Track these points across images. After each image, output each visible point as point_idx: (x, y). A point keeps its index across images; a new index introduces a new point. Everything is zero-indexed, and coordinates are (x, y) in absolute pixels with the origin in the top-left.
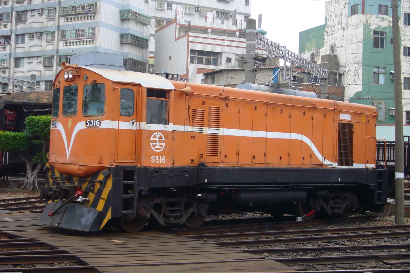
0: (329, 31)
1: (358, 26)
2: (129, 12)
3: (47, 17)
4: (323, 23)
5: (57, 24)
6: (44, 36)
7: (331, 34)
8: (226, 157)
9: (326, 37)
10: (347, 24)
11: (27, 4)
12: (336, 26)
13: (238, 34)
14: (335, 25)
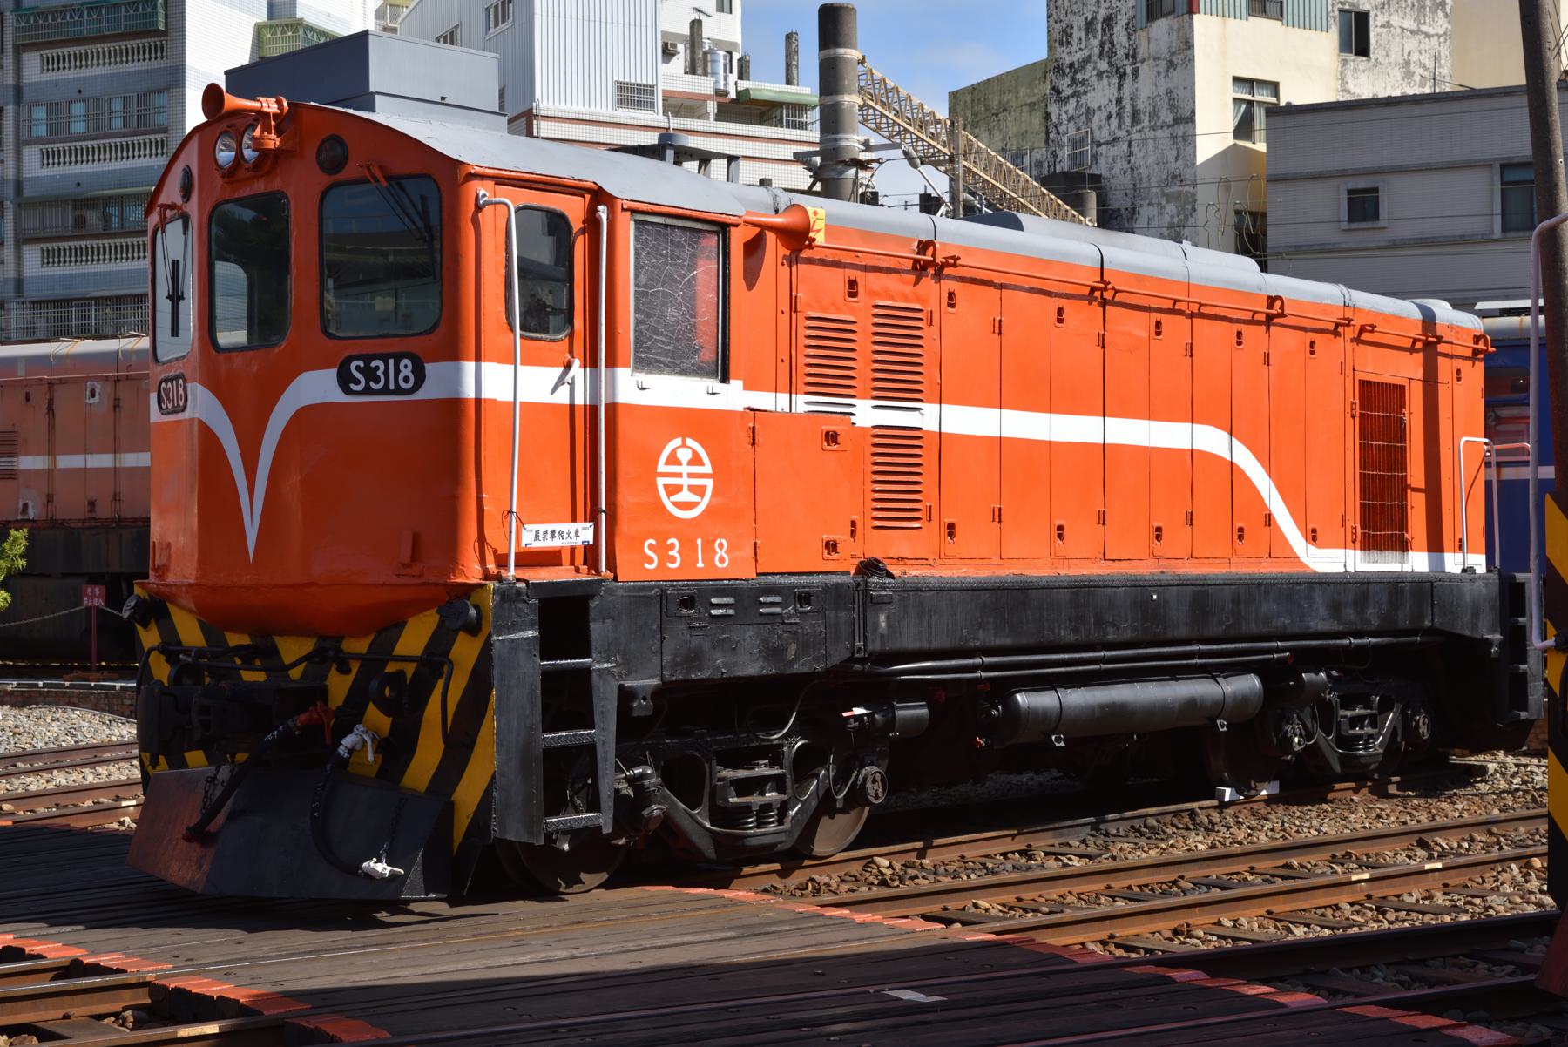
1: (1175, 59)
2: (296, 31)
5: (10, 81)
7: (1072, 96)
10: (1134, 57)
12: (1090, 66)
13: (712, 107)
14: (1088, 59)
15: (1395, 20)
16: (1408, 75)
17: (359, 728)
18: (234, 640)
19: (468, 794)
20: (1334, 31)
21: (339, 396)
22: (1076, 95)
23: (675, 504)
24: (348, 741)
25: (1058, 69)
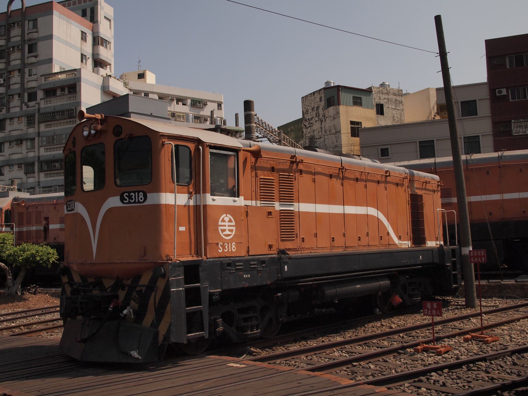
0: (307, 124)
3: (26, 124)
4: (301, 117)
5: (37, 131)
6: (24, 142)
8: (303, 241)
9: (304, 130)
11: (5, 112)
15: (390, 106)
16: (394, 120)
17: (128, 308)
18: (90, 280)
19: (162, 329)
20: (375, 109)
21: (120, 204)
22: (310, 126)
23: (224, 235)
24: (125, 312)
25: (306, 120)
